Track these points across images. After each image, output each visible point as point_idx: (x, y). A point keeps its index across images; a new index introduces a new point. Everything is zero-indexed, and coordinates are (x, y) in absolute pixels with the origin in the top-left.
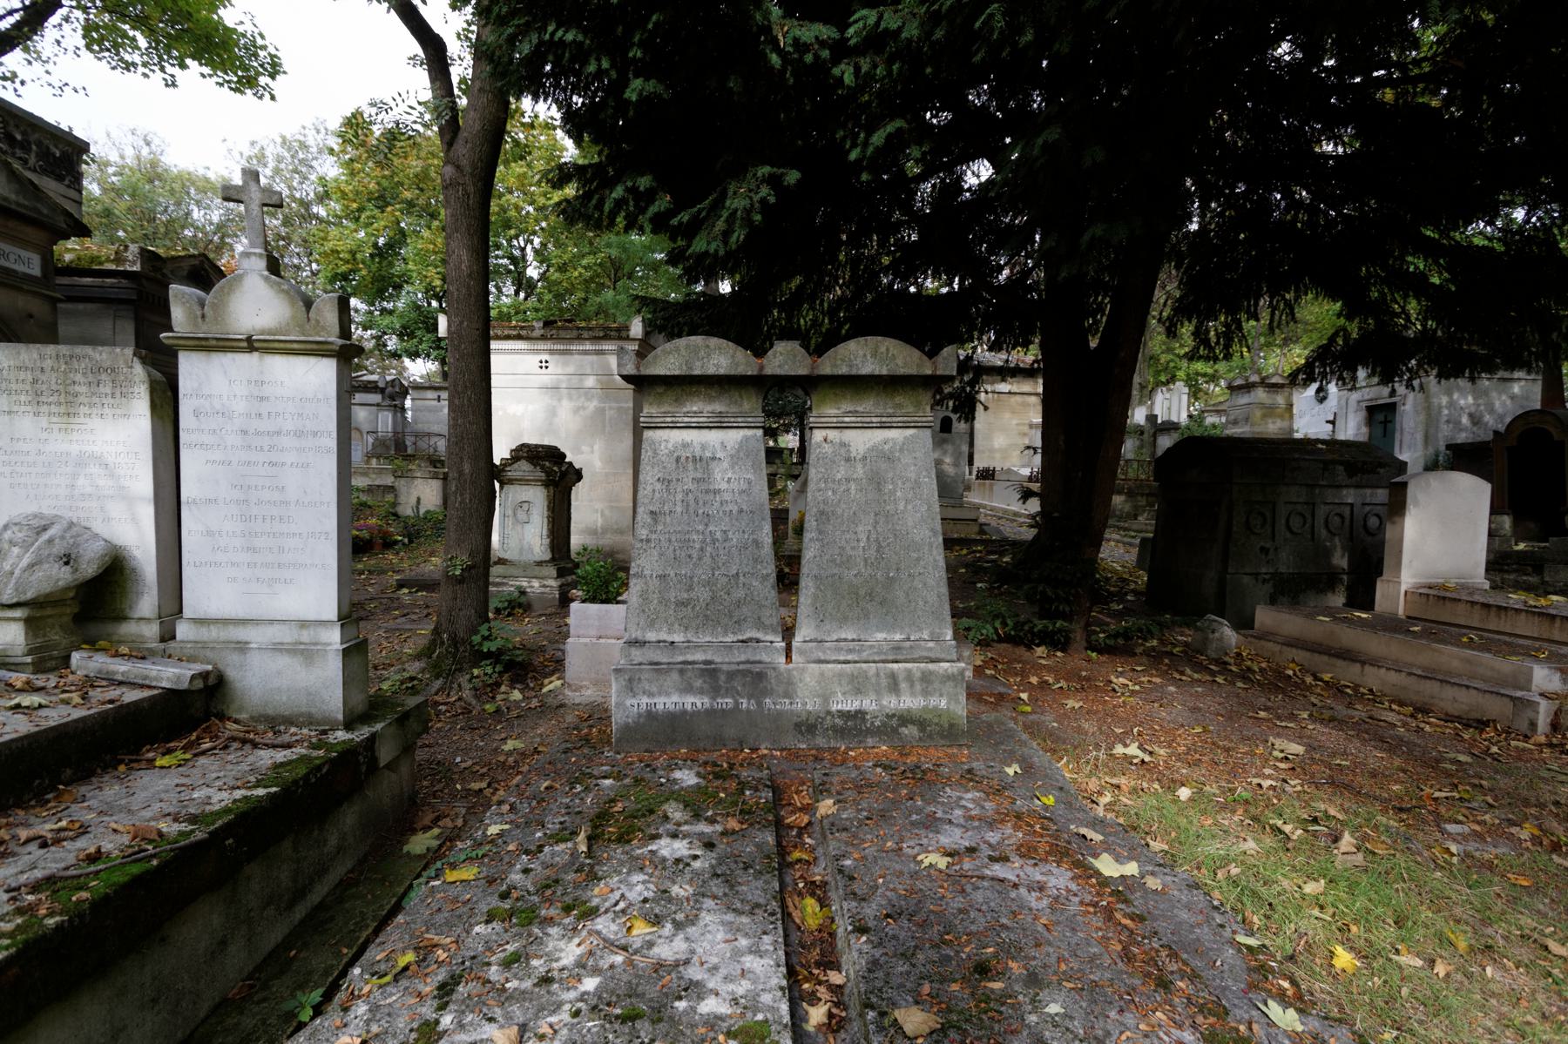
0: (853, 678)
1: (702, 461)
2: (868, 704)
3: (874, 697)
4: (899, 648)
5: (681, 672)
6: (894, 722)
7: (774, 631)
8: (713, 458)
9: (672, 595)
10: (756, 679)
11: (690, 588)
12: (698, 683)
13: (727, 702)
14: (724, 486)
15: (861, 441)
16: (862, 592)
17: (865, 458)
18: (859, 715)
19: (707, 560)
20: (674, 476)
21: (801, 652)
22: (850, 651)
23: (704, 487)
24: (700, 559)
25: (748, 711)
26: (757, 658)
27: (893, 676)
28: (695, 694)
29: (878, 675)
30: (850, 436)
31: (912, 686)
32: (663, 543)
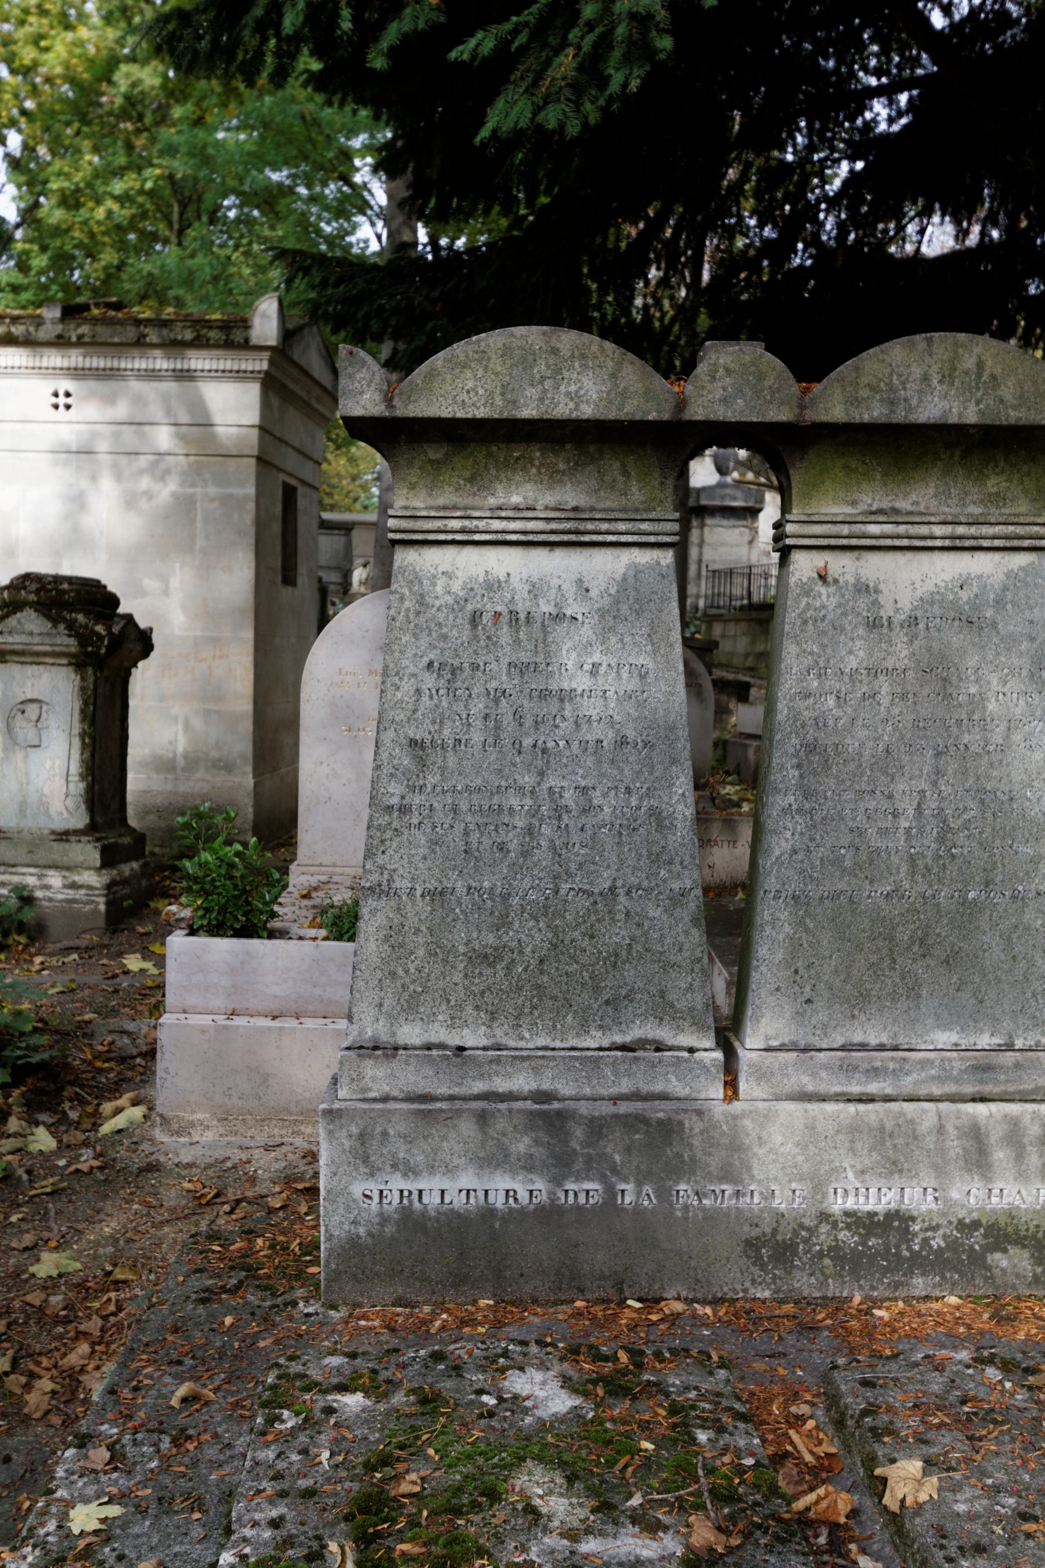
0: (881, 1136)
1: (534, 626)
2: (916, 1198)
3: (930, 1182)
4: (988, 1068)
5: (483, 1118)
6: (977, 1240)
7: (698, 1025)
8: (558, 617)
9: (459, 937)
10: (659, 1137)
11: (503, 923)
12: (522, 1145)
13: (584, 1190)
14: (582, 682)
15: (908, 579)
16: (903, 935)
17: (913, 621)
18: (896, 1222)
19: (542, 855)
20: (466, 659)
21: (761, 1074)
22: (875, 1072)
23: (536, 683)
24: (525, 854)
25: (638, 1211)
26: (658, 1087)
27: (975, 1134)
28: (513, 1172)
29: (941, 1130)
30: (875, 567)
31: (1020, 1156)
32: (440, 816)
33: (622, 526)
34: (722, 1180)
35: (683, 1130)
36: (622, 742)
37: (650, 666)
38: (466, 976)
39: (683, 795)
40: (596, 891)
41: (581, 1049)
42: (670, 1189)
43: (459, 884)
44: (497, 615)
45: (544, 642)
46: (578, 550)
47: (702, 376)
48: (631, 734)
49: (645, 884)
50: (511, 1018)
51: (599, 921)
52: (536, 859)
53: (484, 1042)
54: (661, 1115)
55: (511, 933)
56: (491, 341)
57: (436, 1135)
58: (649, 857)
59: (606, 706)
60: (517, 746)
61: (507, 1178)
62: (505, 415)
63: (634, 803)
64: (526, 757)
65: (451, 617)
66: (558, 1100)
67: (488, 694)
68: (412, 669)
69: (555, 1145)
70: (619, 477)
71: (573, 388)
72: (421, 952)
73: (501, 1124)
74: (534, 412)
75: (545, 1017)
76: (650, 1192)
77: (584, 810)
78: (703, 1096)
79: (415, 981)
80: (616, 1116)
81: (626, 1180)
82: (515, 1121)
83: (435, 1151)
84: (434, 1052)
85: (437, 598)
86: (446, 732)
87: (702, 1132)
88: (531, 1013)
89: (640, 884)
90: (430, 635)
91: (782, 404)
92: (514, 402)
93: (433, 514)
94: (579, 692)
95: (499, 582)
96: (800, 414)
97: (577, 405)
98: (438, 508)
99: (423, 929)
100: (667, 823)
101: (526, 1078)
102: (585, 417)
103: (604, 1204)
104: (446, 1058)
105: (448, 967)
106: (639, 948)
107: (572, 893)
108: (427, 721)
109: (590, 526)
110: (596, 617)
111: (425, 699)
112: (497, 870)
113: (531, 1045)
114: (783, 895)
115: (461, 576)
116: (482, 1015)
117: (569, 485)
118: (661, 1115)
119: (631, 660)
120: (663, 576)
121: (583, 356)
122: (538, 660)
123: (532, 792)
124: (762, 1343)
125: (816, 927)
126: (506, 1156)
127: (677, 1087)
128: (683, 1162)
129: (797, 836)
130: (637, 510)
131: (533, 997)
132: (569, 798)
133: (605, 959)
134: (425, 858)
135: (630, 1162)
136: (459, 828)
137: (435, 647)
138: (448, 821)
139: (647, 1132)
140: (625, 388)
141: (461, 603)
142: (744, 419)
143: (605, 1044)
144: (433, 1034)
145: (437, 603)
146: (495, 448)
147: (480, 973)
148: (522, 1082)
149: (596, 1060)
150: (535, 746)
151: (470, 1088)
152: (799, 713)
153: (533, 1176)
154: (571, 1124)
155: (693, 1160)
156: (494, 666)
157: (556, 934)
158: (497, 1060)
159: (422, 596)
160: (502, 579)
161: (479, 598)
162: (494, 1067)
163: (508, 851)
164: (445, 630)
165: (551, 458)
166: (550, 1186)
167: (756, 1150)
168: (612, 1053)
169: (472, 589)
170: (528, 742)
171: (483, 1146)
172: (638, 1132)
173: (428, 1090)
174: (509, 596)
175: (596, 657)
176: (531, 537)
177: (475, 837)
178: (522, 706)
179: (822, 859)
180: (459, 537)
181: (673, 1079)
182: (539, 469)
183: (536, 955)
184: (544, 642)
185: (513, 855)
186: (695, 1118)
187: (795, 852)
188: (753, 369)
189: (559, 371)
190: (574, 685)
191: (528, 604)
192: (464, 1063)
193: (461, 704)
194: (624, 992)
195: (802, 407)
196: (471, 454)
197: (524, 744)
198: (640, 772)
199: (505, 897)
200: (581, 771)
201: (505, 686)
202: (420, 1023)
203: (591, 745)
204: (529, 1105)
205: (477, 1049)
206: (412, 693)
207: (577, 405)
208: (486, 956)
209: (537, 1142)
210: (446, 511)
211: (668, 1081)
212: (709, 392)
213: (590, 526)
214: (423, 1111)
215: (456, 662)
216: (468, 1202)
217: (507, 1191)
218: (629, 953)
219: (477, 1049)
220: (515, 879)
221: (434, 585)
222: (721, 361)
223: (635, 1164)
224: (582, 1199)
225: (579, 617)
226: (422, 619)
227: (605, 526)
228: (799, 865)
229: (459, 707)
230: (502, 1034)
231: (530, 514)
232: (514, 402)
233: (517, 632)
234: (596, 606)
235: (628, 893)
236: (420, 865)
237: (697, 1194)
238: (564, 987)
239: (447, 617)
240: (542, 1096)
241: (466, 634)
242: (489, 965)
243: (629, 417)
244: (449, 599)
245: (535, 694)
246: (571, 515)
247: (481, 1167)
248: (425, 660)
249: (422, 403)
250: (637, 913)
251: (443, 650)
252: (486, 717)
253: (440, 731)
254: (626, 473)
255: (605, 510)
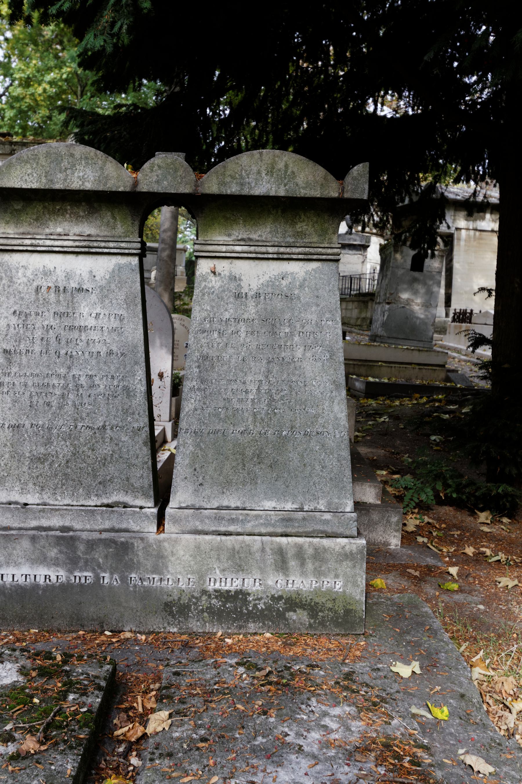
0: (233, 553)
1: (70, 293)
2: (250, 583)
3: (258, 576)
4: (289, 520)
5: (33, 539)
6: (281, 605)
7: (145, 495)
8: (80, 290)
9: (27, 449)
10: (120, 550)
11: (48, 442)
12: (53, 553)
13: (85, 576)
14: (91, 322)
15: (255, 275)
16: (249, 453)
17: (258, 295)
18: (240, 596)
19: (69, 409)
20: (33, 309)
21: (176, 521)
22: (233, 521)
23: (67, 322)
24: (60, 408)
25: (111, 587)
26: (124, 526)
27: (281, 552)
28: (48, 566)
29: (263, 550)
30: (242, 268)
31: (303, 564)
32: (18, 388)
33: (111, 245)
34: (153, 572)
35: (134, 547)
36: (110, 353)
37: (125, 315)
38: (29, 468)
39: (140, 380)
40: (96, 427)
41: (86, 506)
42: (127, 576)
43: (27, 422)
44: (49, 288)
45: (72, 302)
46: (91, 256)
47: (147, 169)
48: (115, 349)
49: (120, 424)
50: (51, 490)
51: (96, 442)
52: (65, 411)
53: (38, 501)
54: (123, 539)
55: (52, 447)
56: (40, 149)
57: (10, 547)
58: (122, 411)
59: (102, 335)
60: (57, 354)
61: (46, 569)
62: (47, 187)
63: (115, 383)
64: (62, 359)
65: (26, 288)
66: (73, 531)
67: (44, 327)
68: (5, 314)
69: (69, 553)
70: (111, 220)
71: (81, 174)
72: (7, 456)
73: (43, 542)
74: (62, 186)
75: (69, 489)
76: (117, 578)
77: (90, 387)
78: (146, 530)
79: (3, 470)
80: (100, 540)
81: (105, 572)
82: (50, 541)
83: (10, 555)
84: (12, 506)
85: (19, 279)
86: (22, 346)
87: (143, 548)
88: (62, 487)
89: (118, 424)
90: (15, 297)
91: (186, 184)
92: (52, 181)
93: (17, 236)
94: (89, 327)
95: (50, 271)
96: (196, 190)
97: (83, 183)
98: (17, 234)
99: (8, 444)
100: (132, 394)
101: (57, 520)
102: (87, 189)
103: (94, 583)
104: (18, 509)
105: (20, 464)
106: (117, 456)
107: (83, 428)
108: (12, 340)
109: (95, 244)
110: (99, 290)
111: (12, 329)
112: (46, 416)
113: (61, 503)
114: (190, 431)
115: (31, 268)
116: (37, 488)
117: (86, 223)
118: (123, 539)
119: (116, 312)
120: (133, 270)
121: (86, 158)
122: (69, 311)
123: (64, 377)
124: (163, 653)
125: (205, 447)
126: (45, 558)
127: (133, 526)
128: (134, 563)
129: (197, 402)
130: (120, 237)
131: (63, 479)
132: (83, 380)
133: (99, 461)
134: (10, 409)
135: (107, 563)
136: (27, 394)
137: (17, 304)
138: (22, 391)
139: (116, 548)
140: (107, 175)
141: (31, 281)
142: (167, 192)
143: (99, 503)
144: (12, 497)
145: (19, 281)
146: (47, 204)
147: (37, 467)
148: (56, 521)
149: (93, 512)
150: (66, 354)
151: (29, 524)
152: (200, 340)
153: (58, 569)
154: (77, 543)
155: (138, 562)
156: (46, 314)
157: (75, 448)
158: (43, 511)
159: (11, 277)
160: (52, 270)
161: (40, 279)
162: (41, 514)
163: (52, 406)
164: (22, 295)
165: (76, 210)
166: (67, 574)
167: (170, 558)
168: (101, 508)
169: (36, 275)
170: (63, 352)
171: (33, 553)
172: (111, 548)
173: (8, 525)
174: (55, 279)
175: (98, 310)
176: (65, 249)
177: (35, 399)
178: (60, 334)
179: (209, 414)
180: (29, 248)
181: (131, 522)
182: (70, 215)
183: (65, 458)
184: (72, 302)
185: (54, 408)
186: (140, 541)
187: (196, 410)
188: (172, 166)
189: (74, 165)
190: (87, 324)
191: (64, 283)
192: (26, 512)
193: (30, 332)
194: (108, 478)
195: (197, 186)
196: (36, 207)
197: (61, 353)
198: (119, 368)
199: (50, 429)
200: (89, 367)
201: (52, 324)
202: (6, 491)
203: (95, 354)
204: (58, 533)
205: (34, 504)
206: (5, 326)
207: (83, 183)
208: (39, 459)
209: (61, 552)
210: (23, 235)
211: (129, 522)
212: (150, 178)
213: (95, 244)
214: (3, 535)
215: (28, 311)
216: (26, 581)
217: (46, 576)
218: (111, 458)
219: (34, 504)
220: (55, 420)
221: (18, 272)
222: (156, 162)
223: (109, 563)
224: (83, 580)
225: (90, 290)
226: (11, 289)
227: (103, 244)
228: (198, 417)
229: (29, 334)
230: (47, 498)
231: (65, 237)
232: (52, 181)
233: (59, 297)
234: (99, 284)
235: (112, 428)
236: (8, 412)
237: (141, 579)
238: (79, 475)
239: (24, 288)
240: (64, 529)
241: (33, 297)
242: (41, 463)
243: (110, 189)
244: (25, 280)
245: (67, 328)
246: (86, 238)
247: (33, 564)
248: (12, 310)
249: (5, 180)
250: (116, 439)
251: (21, 305)
252: (42, 339)
253: (19, 346)
254: (114, 218)
255: (104, 236)
